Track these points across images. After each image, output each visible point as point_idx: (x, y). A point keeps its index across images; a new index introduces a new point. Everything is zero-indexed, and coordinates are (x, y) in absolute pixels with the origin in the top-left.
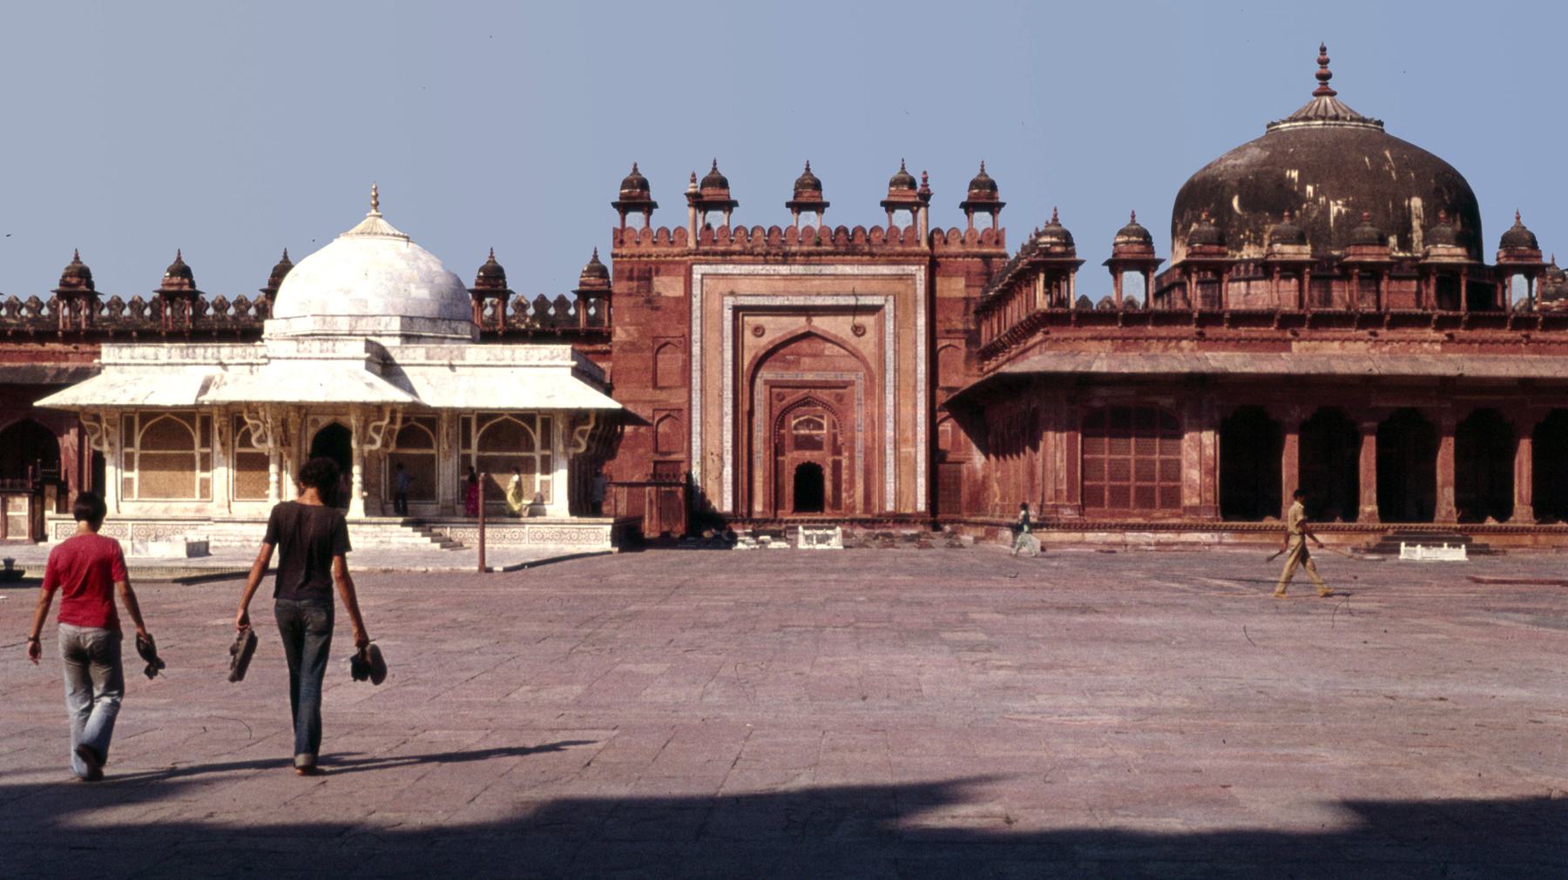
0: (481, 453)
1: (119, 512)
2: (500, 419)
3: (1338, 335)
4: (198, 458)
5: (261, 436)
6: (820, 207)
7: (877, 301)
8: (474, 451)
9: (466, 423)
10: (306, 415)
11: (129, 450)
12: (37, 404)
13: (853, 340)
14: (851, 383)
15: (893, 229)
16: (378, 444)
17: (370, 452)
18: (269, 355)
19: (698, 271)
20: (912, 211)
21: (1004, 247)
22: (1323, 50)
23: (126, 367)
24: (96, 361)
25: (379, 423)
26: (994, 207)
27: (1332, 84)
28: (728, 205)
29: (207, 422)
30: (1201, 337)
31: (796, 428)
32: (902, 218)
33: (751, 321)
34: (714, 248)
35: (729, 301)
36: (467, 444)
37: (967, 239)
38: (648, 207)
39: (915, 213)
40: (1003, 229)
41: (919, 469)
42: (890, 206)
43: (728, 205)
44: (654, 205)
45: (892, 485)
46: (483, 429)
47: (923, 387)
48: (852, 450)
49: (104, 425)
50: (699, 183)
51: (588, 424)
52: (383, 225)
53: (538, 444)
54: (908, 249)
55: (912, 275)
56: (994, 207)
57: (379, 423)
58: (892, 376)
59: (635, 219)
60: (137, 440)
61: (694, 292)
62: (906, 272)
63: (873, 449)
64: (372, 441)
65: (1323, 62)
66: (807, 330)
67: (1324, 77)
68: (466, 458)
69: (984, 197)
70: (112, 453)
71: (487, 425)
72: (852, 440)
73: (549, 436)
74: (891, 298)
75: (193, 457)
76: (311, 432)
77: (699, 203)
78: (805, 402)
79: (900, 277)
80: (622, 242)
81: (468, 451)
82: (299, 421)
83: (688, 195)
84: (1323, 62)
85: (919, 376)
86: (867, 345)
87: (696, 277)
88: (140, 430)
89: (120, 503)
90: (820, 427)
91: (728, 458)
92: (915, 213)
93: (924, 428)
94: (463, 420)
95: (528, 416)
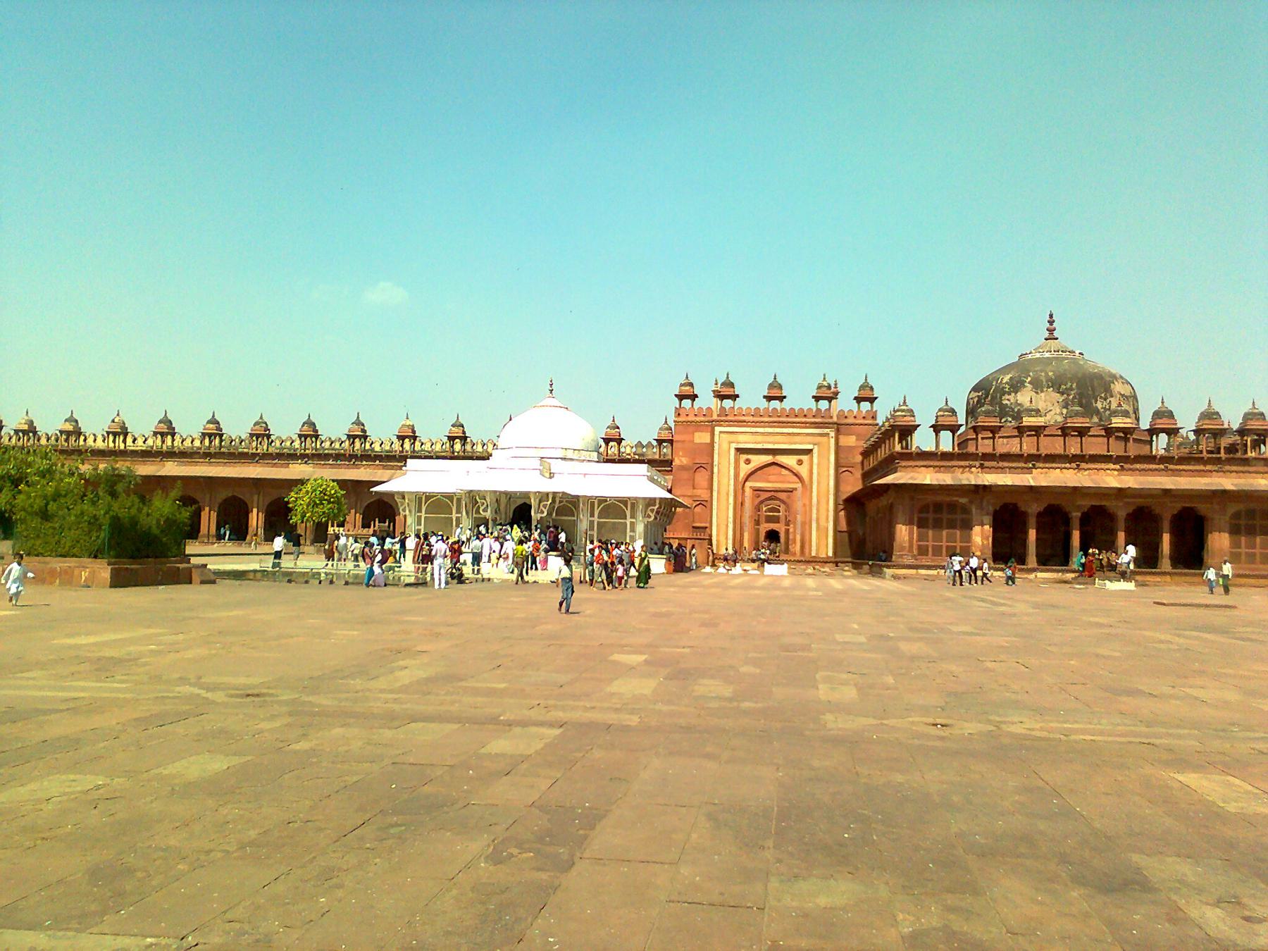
3: (1059, 465)
4: (454, 519)
6: (781, 399)
7: (810, 447)
8: (596, 519)
9: (593, 504)
11: (418, 514)
12: (371, 490)
13: (797, 468)
14: (796, 489)
15: (818, 410)
16: (545, 514)
17: (541, 517)
19: (717, 429)
21: (876, 420)
22: (1051, 316)
25: (546, 503)
26: (872, 400)
27: (1056, 334)
28: (734, 397)
29: (459, 500)
30: (982, 466)
31: (765, 512)
32: (824, 405)
33: (744, 457)
34: (725, 418)
35: (734, 446)
36: (592, 515)
38: (693, 397)
39: (830, 402)
40: (876, 411)
42: (817, 399)
43: (734, 397)
44: (696, 396)
48: (795, 523)
49: (407, 501)
50: (719, 385)
51: (655, 506)
53: (628, 516)
54: (826, 421)
55: (829, 434)
56: (872, 400)
57: (546, 503)
59: (687, 403)
61: (715, 441)
65: (1051, 322)
66: (772, 461)
67: (1051, 331)
68: (592, 523)
69: (866, 396)
70: (411, 516)
71: (603, 505)
72: (796, 518)
75: (451, 519)
76: (513, 508)
77: (721, 397)
78: (770, 499)
80: (679, 414)
83: (714, 391)
84: (1051, 322)
86: (803, 471)
87: (717, 433)
90: (780, 512)
91: (731, 526)
92: (830, 402)
94: (591, 502)
95: (624, 501)
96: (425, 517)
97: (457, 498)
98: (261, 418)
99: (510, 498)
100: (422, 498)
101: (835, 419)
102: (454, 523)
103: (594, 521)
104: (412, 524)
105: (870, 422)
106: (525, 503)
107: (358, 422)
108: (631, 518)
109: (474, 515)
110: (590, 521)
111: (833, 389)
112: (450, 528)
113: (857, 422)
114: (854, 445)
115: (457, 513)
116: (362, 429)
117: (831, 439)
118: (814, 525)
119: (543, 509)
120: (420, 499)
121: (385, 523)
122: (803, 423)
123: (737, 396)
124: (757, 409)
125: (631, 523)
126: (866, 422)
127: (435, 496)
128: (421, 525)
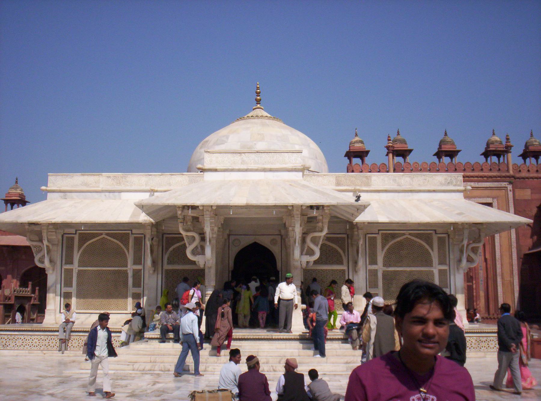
2: (401, 238)
4: (130, 274)
5: (196, 247)
8: (380, 267)
9: (373, 242)
11: (68, 267)
16: (317, 256)
23: (68, 194)
24: (43, 188)
29: (139, 242)
36: (373, 261)
41: (515, 289)
45: (502, 298)
46: (387, 247)
47: (515, 246)
49: (45, 242)
53: (435, 259)
54: (504, 174)
55: (507, 187)
58: (499, 240)
62: (502, 186)
64: (311, 252)
70: (53, 270)
74: (495, 200)
75: (126, 272)
76: (235, 250)
79: (499, 188)
81: (373, 267)
85: (512, 240)
93: (516, 267)
96: (80, 273)
99: (229, 235)
100: (73, 239)
101: (511, 172)
102: (130, 281)
103: (376, 271)
104: (55, 283)
106: (255, 242)
108: (439, 264)
109: (167, 267)
113: (532, 175)
114: (529, 198)
115: (135, 263)
119: (312, 246)
120: (71, 240)
122: (481, 177)
123: (410, 151)
125: (440, 271)
128: (71, 286)
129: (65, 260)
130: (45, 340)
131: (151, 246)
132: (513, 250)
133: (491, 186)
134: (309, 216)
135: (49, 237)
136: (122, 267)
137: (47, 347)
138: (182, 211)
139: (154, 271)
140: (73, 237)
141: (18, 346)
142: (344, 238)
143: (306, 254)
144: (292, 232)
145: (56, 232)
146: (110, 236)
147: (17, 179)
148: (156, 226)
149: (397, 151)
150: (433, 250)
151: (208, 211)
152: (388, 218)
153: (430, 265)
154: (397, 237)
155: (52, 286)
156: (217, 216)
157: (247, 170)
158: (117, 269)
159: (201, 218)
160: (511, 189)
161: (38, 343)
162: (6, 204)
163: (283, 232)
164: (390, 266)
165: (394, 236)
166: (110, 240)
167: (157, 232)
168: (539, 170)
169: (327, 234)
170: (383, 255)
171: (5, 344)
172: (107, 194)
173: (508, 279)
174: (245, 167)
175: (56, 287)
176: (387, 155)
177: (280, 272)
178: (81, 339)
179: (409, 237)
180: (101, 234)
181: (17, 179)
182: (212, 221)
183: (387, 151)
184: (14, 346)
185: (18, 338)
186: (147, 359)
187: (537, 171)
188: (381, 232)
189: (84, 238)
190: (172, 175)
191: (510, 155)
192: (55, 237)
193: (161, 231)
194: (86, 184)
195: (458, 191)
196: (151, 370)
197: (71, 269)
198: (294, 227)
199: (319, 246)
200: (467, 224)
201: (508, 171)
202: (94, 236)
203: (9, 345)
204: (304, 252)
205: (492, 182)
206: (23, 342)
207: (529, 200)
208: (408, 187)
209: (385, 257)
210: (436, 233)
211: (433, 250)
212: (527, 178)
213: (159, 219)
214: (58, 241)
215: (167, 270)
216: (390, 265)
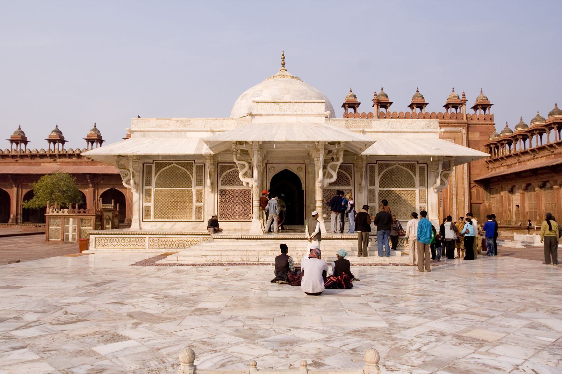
0: (381, 189)
1: (141, 229)
2: (393, 167)
8: (377, 188)
9: (372, 170)
10: (267, 164)
11: (148, 187)
15: (452, 113)
18: (254, 113)
20: (455, 109)
21: (493, 121)
23: (147, 133)
26: (485, 106)
29: (201, 169)
36: (373, 184)
37: (479, 118)
40: (493, 115)
45: (456, 212)
47: (467, 175)
49: (131, 170)
52: (287, 73)
55: (461, 131)
59: (351, 110)
60: (154, 180)
62: (458, 130)
63: (447, 198)
68: (372, 193)
70: (137, 190)
71: (386, 170)
73: (424, 177)
75: (191, 192)
76: (271, 176)
82: (263, 167)
83: (373, 100)
88: (156, 174)
89: (142, 223)
93: (467, 190)
96: (156, 192)
97: (197, 165)
98: (20, 128)
99: (267, 164)
100: (151, 167)
105: (489, 122)
107: (95, 130)
109: (221, 187)
110: (370, 190)
111: (461, 98)
112: (187, 204)
113: (480, 122)
114: (479, 139)
116: (98, 135)
117: (463, 135)
118: (454, 200)
121: (111, 204)
123: (391, 103)
124: (408, 113)
126: (487, 122)
127: (167, 164)
129: (146, 182)
130: (134, 241)
131: (210, 172)
132: (465, 178)
133: (450, 130)
134: (329, 149)
135: (134, 166)
136: (188, 187)
137: (135, 246)
138: (236, 146)
139: (212, 190)
140: (152, 165)
141: (114, 245)
142: (351, 166)
143: (327, 178)
144: (317, 161)
145: (138, 162)
146: (179, 165)
147: (95, 123)
148: (214, 157)
149: (381, 103)
150: (415, 176)
151: (256, 145)
152: (385, 152)
153: (413, 186)
154: (390, 166)
155: (136, 202)
156: (261, 150)
157: (283, 115)
158: (184, 189)
159: (250, 151)
160: (465, 132)
161: (128, 243)
162: (88, 142)
163: (307, 161)
164: (384, 187)
165: (387, 165)
166: (178, 168)
167: (214, 162)
168: (486, 118)
169: (342, 163)
170: (379, 179)
171: (104, 244)
172: (176, 133)
173: (460, 199)
174: (282, 113)
175: (139, 202)
176: (373, 106)
177: (304, 191)
178: (160, 240)
179: (399, 166)
180: (172, 164)
181: (95, 123)
182: (258, 153)
183: (374, 103)
184: (111, 245)
185: (114, 240)
186: (216, 253)
187: (484, 119)
188: (378, 162)
189: (159, 166)
190: (224, 119)
191: (464, 106)
192: (138, 166)
193: (216, 161)
194: (160, 127)
195: (435, 132)
196: (219, 261)
197: (150, 189)
198: (320, 158)
199: (337, 172)
200: (441, 156)
201: (463, 119)
202: (167, 164)
203: (107, 244)
204: (326, 176)
205: (452, 127)
206: (117, 243)
207: (478, 141)
208: (399, 130)
209: (381, 180)
210: (418, 163)
211: (415, 176)
212: (477, 124)
213: (217, 152)
214: (140, 169)
215: (221, 190)
216: (384, 186)
